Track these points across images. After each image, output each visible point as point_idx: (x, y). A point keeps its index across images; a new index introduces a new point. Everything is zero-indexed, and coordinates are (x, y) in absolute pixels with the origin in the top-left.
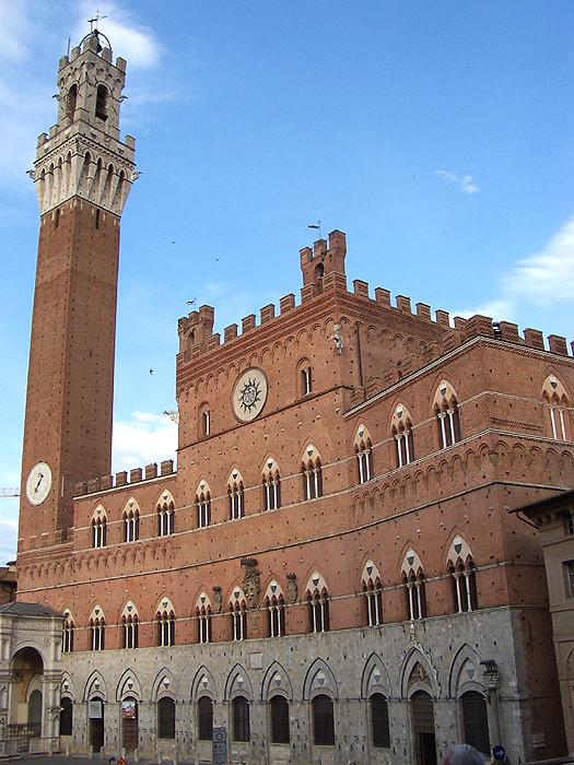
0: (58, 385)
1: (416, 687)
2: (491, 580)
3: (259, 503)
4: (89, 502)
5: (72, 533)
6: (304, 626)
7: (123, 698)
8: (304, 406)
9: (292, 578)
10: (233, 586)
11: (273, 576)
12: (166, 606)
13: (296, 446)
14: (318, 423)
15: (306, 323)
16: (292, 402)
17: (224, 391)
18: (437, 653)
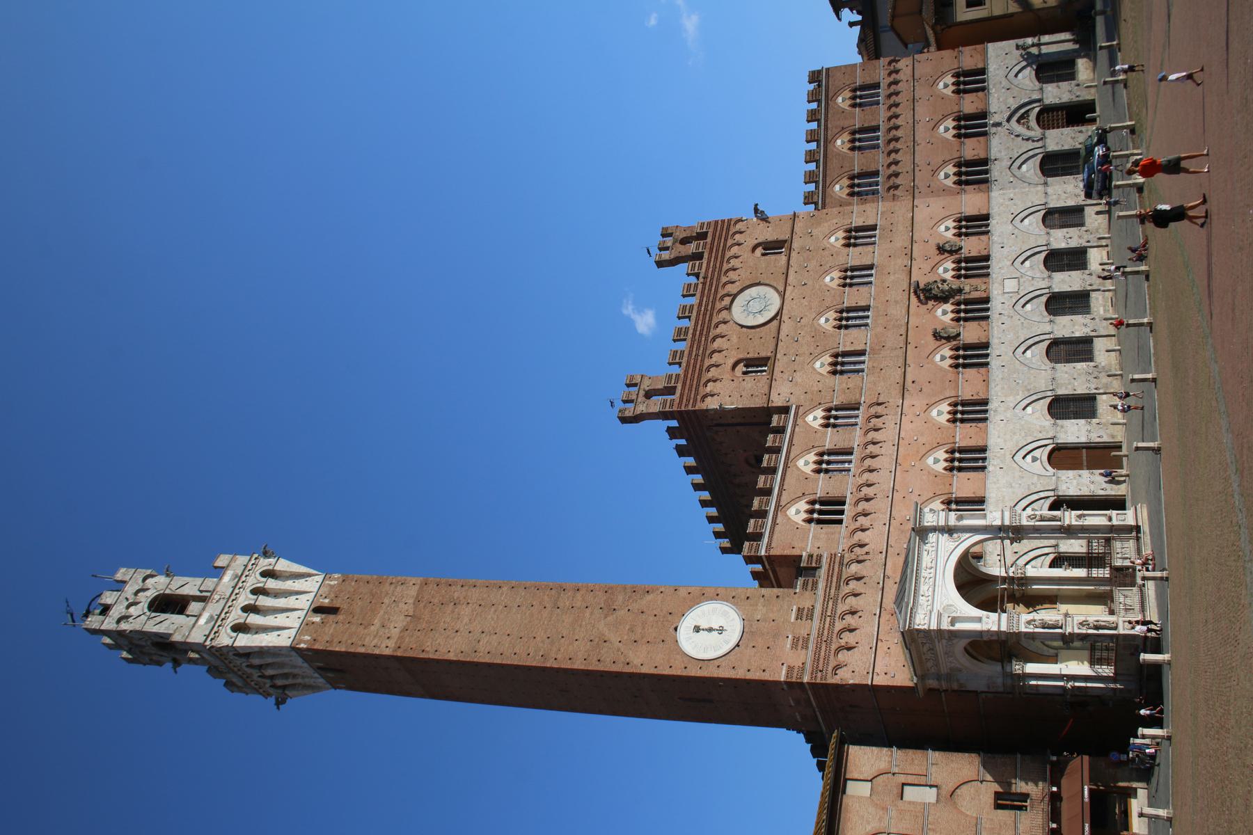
0: (579, 595)
1: (1033, 123)
2: (968, 58)
3: (863, 289)
4: (777, 528)
5: (811, 556)
6: (983, 237)
7: (1049, 468)
8: (795, 245)
9: (941, 249)
10: (936, 317)
11: (934, 268)
12: (940, 414)
13: (826, 252)
14: (815, 232)
15: (725, 245)
16: (783, 258)
17: (734, 339)
18: (1011, 101)
